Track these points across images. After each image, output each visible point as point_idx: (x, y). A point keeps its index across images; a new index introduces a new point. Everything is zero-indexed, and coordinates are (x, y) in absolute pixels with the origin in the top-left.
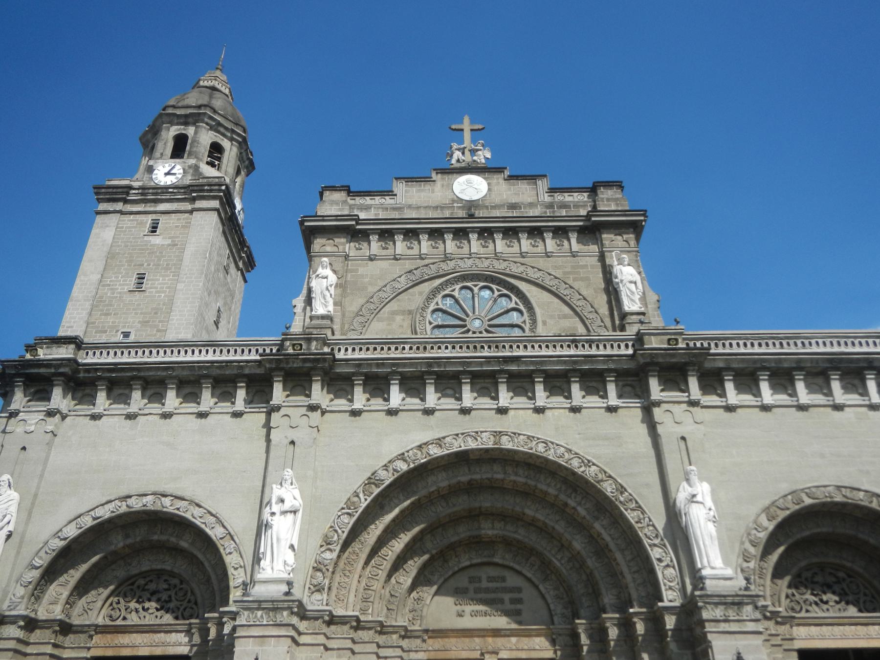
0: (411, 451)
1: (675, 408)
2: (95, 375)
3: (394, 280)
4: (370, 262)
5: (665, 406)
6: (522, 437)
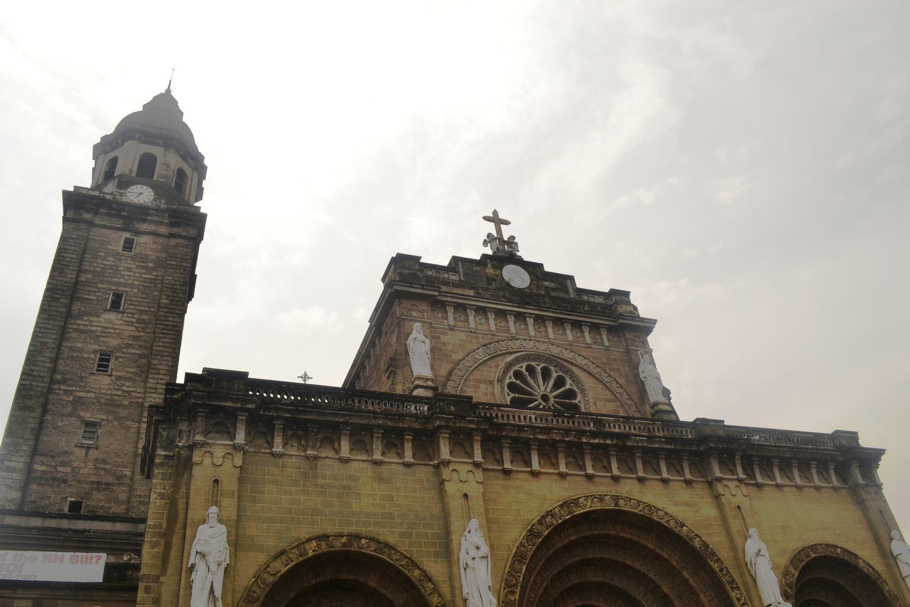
0: (556, 509)
1: (730, 484)
2: (275, 415)
3: (474, 351)
4: (449, 332)
5: (724, 483)
6: (632, 500)
